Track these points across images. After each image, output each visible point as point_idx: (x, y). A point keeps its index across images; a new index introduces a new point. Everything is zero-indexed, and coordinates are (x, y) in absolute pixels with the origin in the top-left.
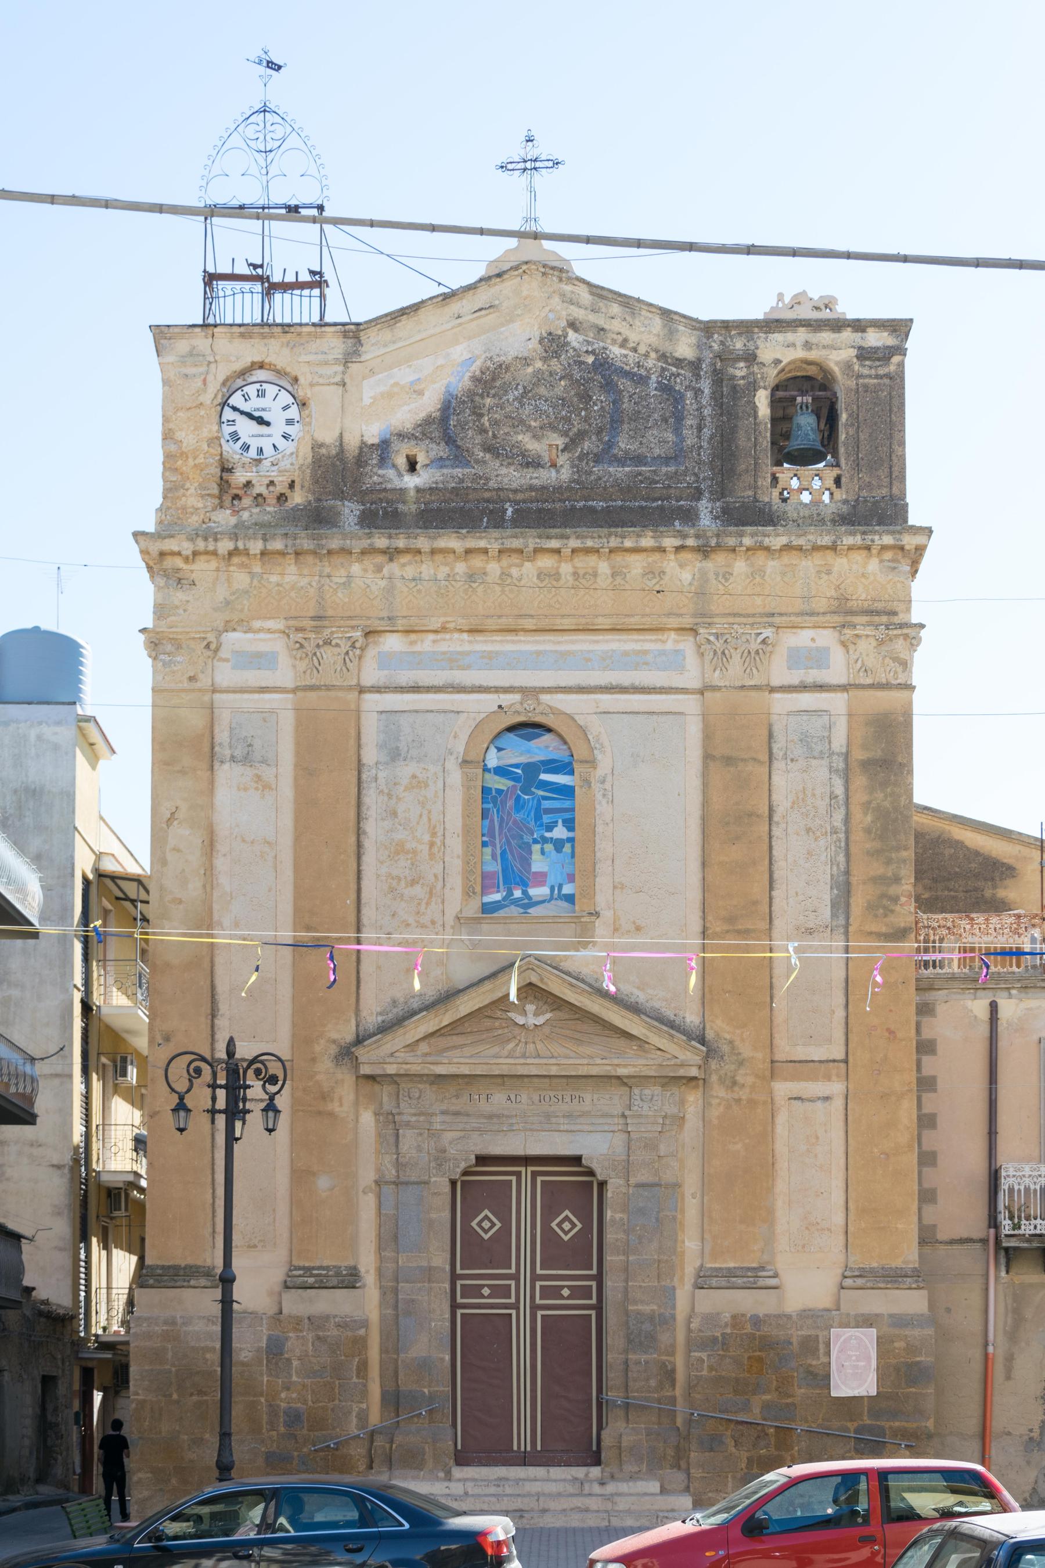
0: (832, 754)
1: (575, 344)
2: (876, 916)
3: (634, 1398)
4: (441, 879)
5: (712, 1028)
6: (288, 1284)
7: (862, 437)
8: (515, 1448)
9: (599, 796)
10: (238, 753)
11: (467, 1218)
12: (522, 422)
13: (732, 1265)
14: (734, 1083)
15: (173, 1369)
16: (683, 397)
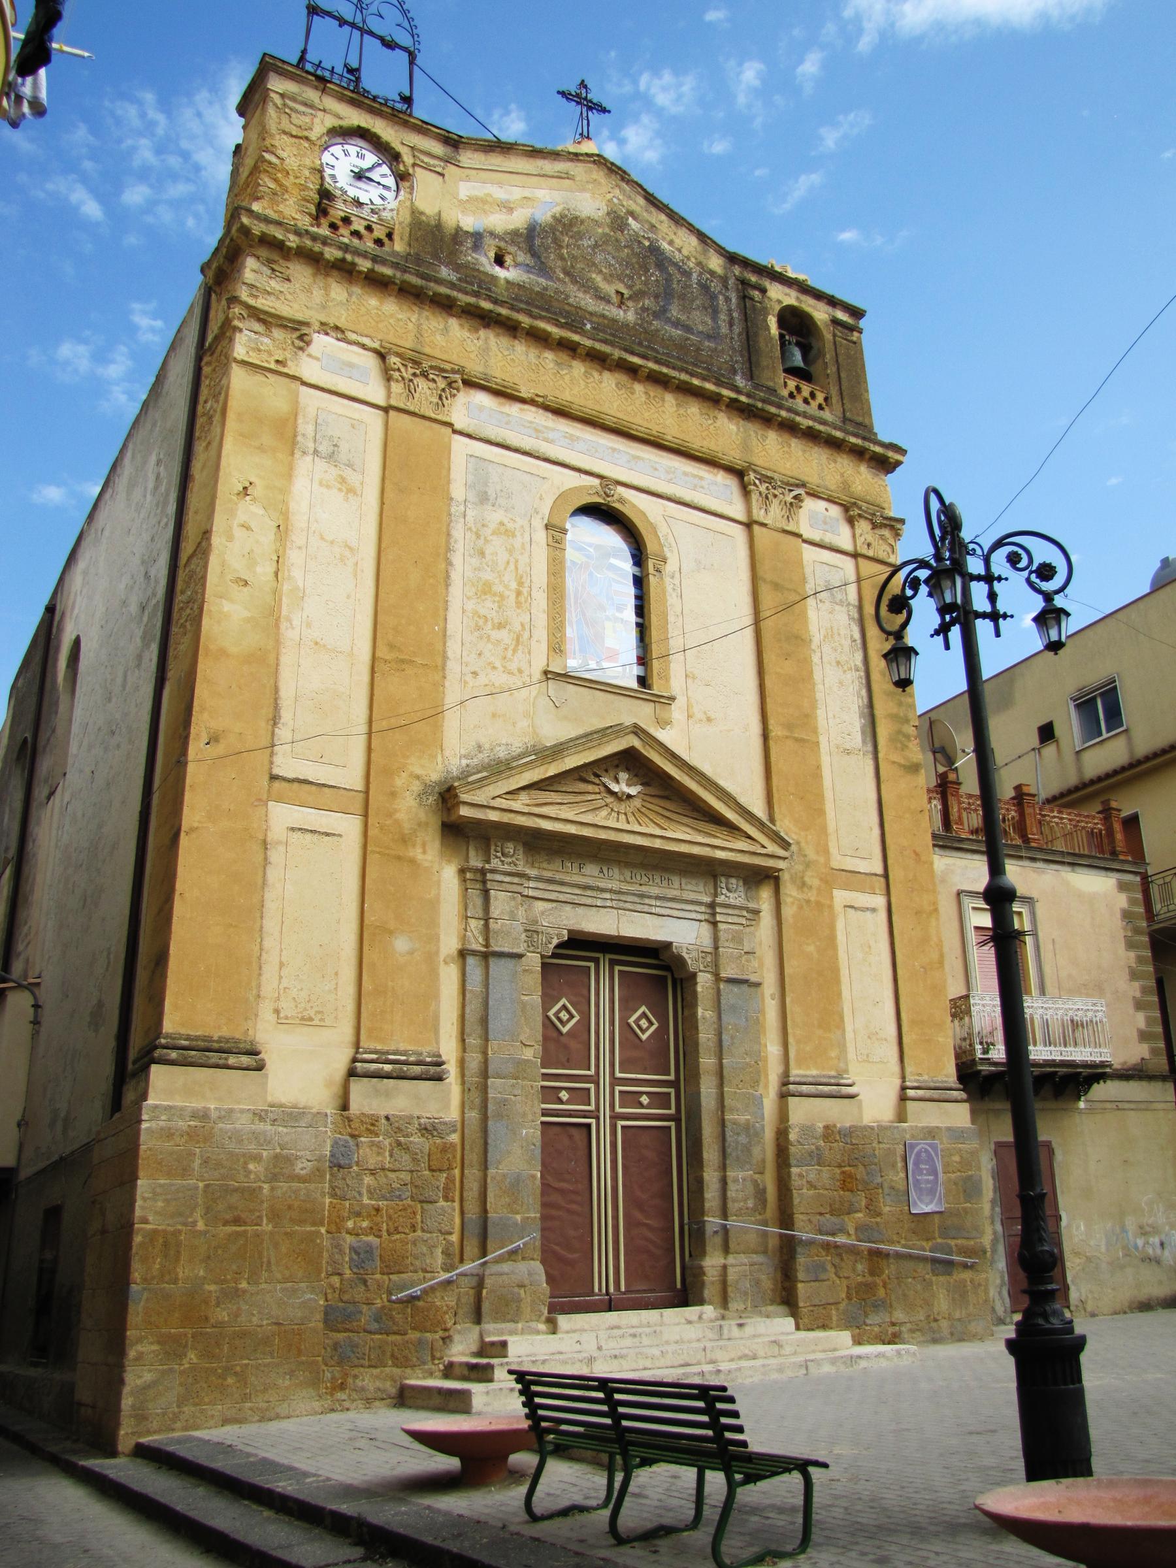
0: (849, 604)
2: (896, 748)
4: (527, 627)
6: (359, 1070)
9: (669, 588)
10: (324, 448)
12: (594, 264)
13: (814, 1072)
14: (804, 884)
15: (201, 1185)
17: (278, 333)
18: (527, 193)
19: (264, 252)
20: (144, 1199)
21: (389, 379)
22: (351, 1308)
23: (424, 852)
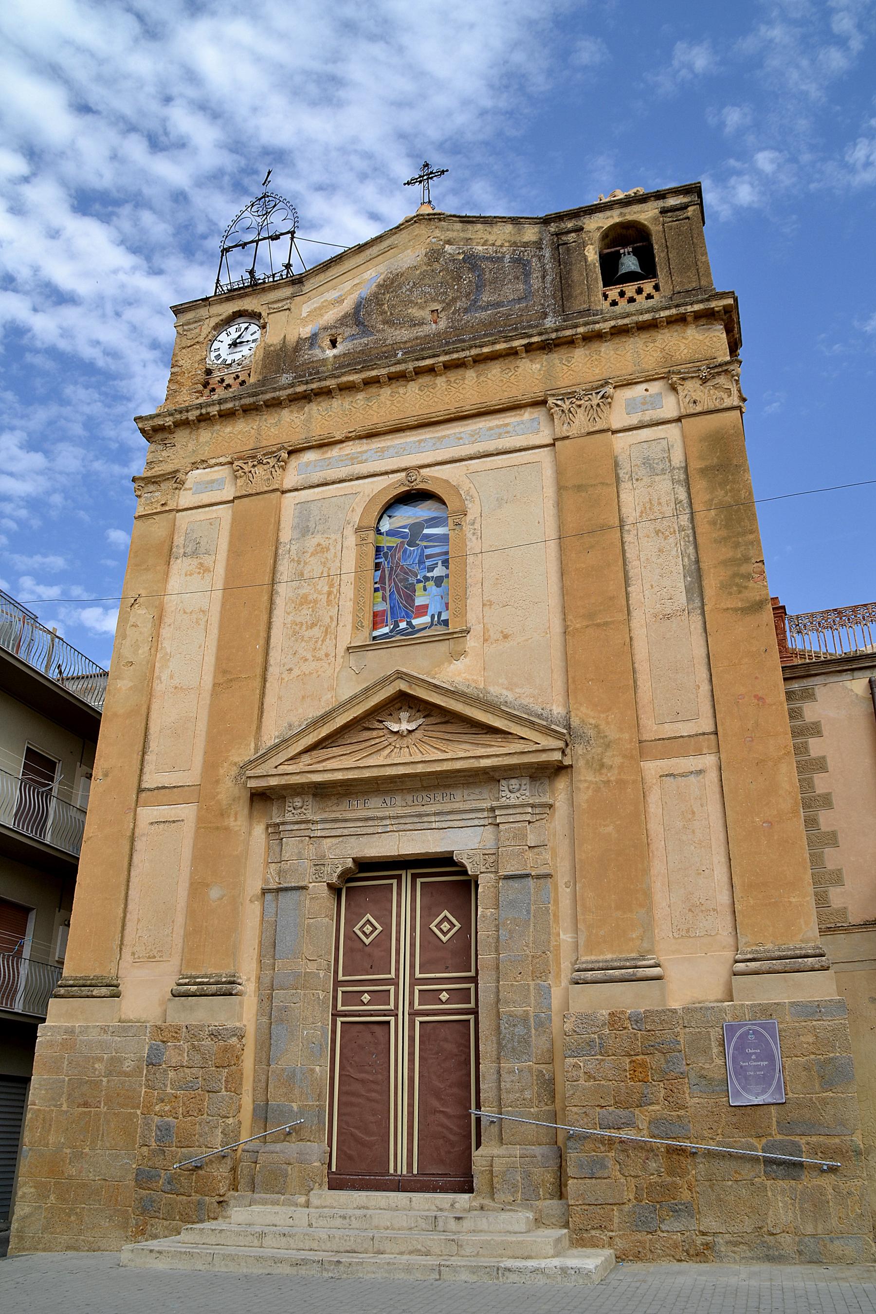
1: (450, 251)
3: (508, 1113)
5: (577, 715)
7: (671, 256)
8: (392, 1171)
10: (189, 550)
11: (350, 924)
12: (411, 302)
13: (609, 956)
14: (602, 766)
15: (67, 1079)
16: (529, 262)
17: (164, 486)
18: (356, 281)
19: (159, 436)
20: (35, 1089)
21: (236, 477)
22: (153, 1172)
23: (236, 820)
